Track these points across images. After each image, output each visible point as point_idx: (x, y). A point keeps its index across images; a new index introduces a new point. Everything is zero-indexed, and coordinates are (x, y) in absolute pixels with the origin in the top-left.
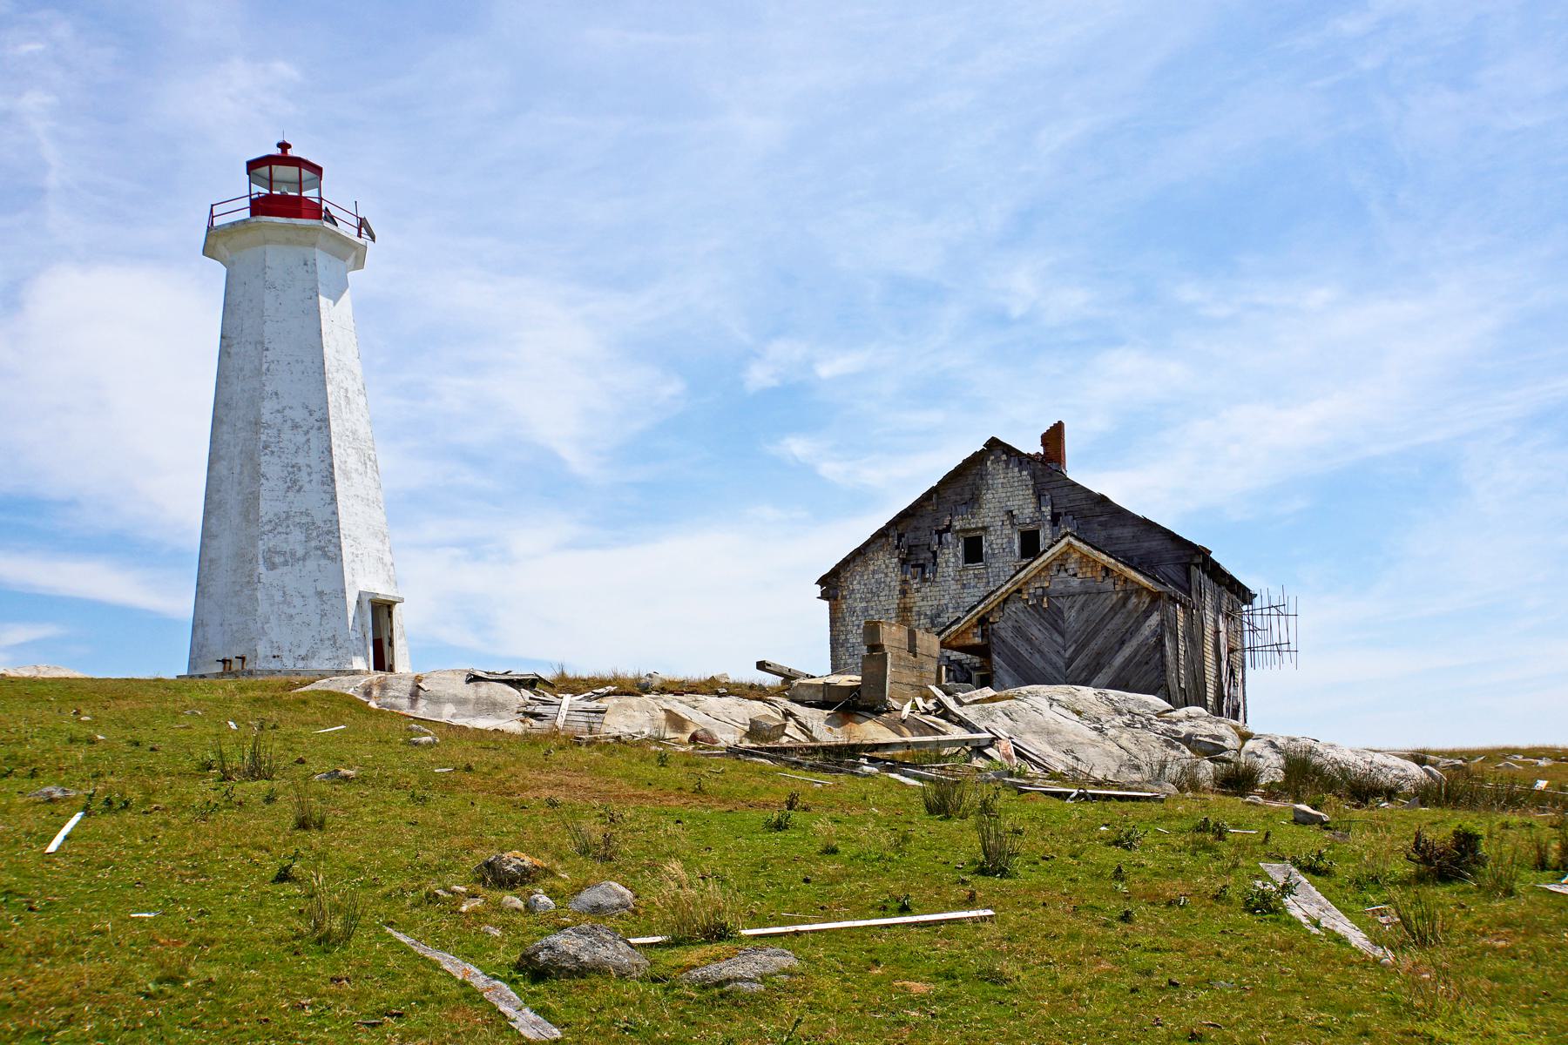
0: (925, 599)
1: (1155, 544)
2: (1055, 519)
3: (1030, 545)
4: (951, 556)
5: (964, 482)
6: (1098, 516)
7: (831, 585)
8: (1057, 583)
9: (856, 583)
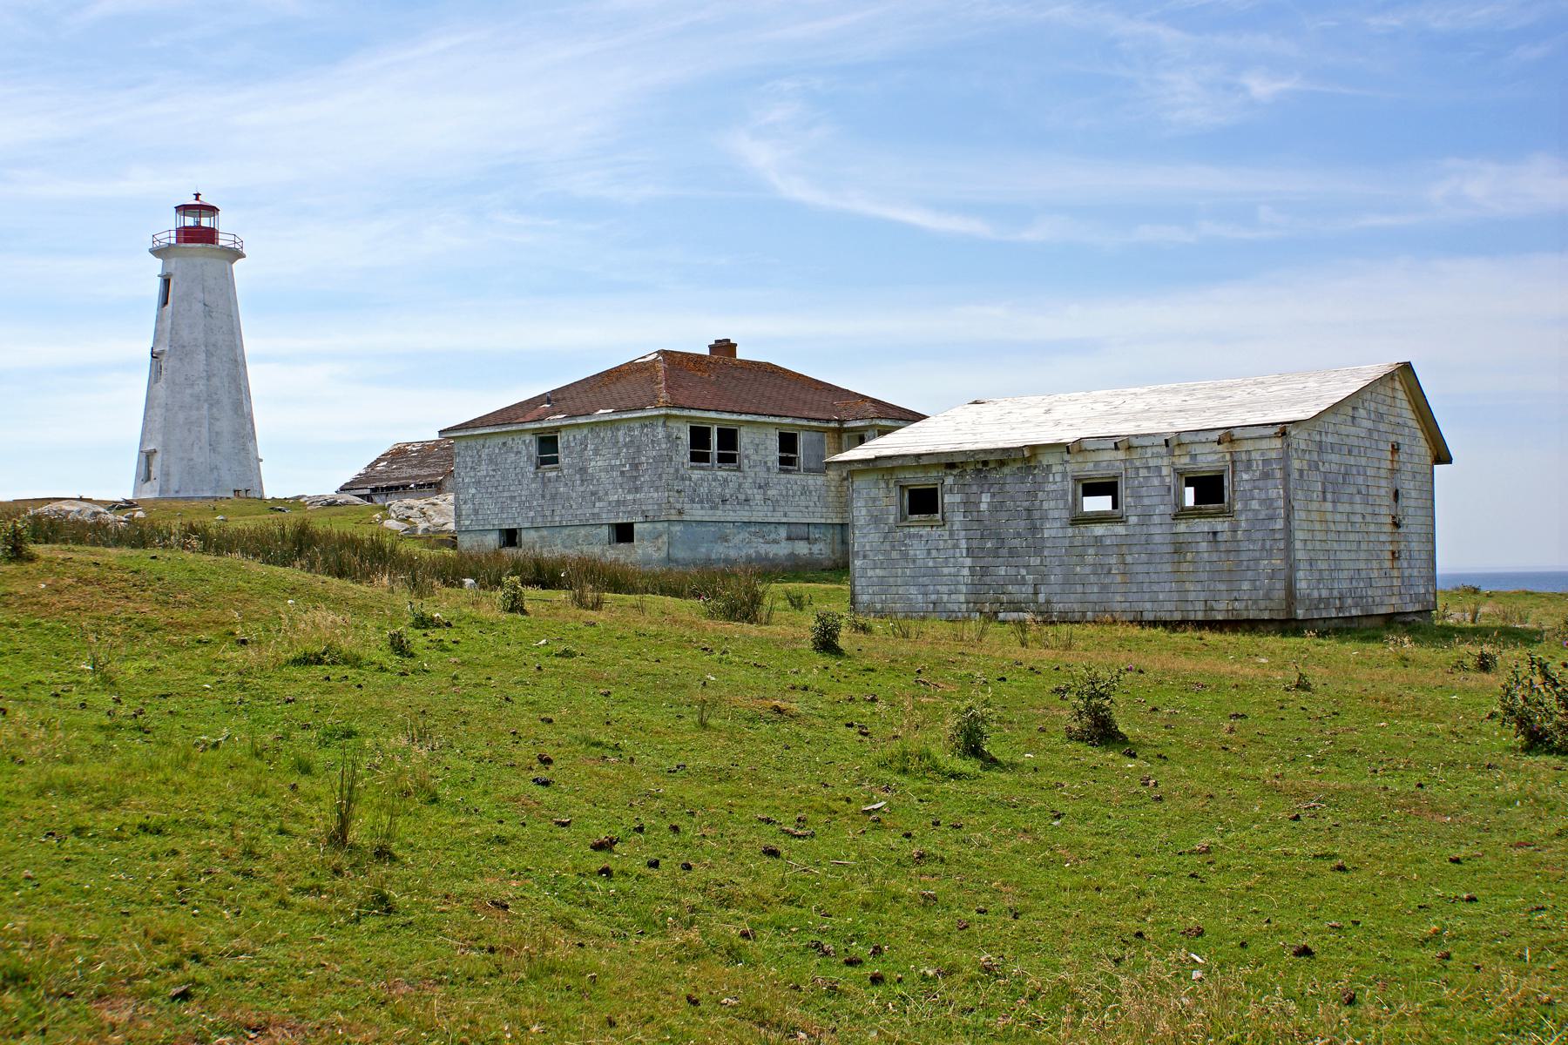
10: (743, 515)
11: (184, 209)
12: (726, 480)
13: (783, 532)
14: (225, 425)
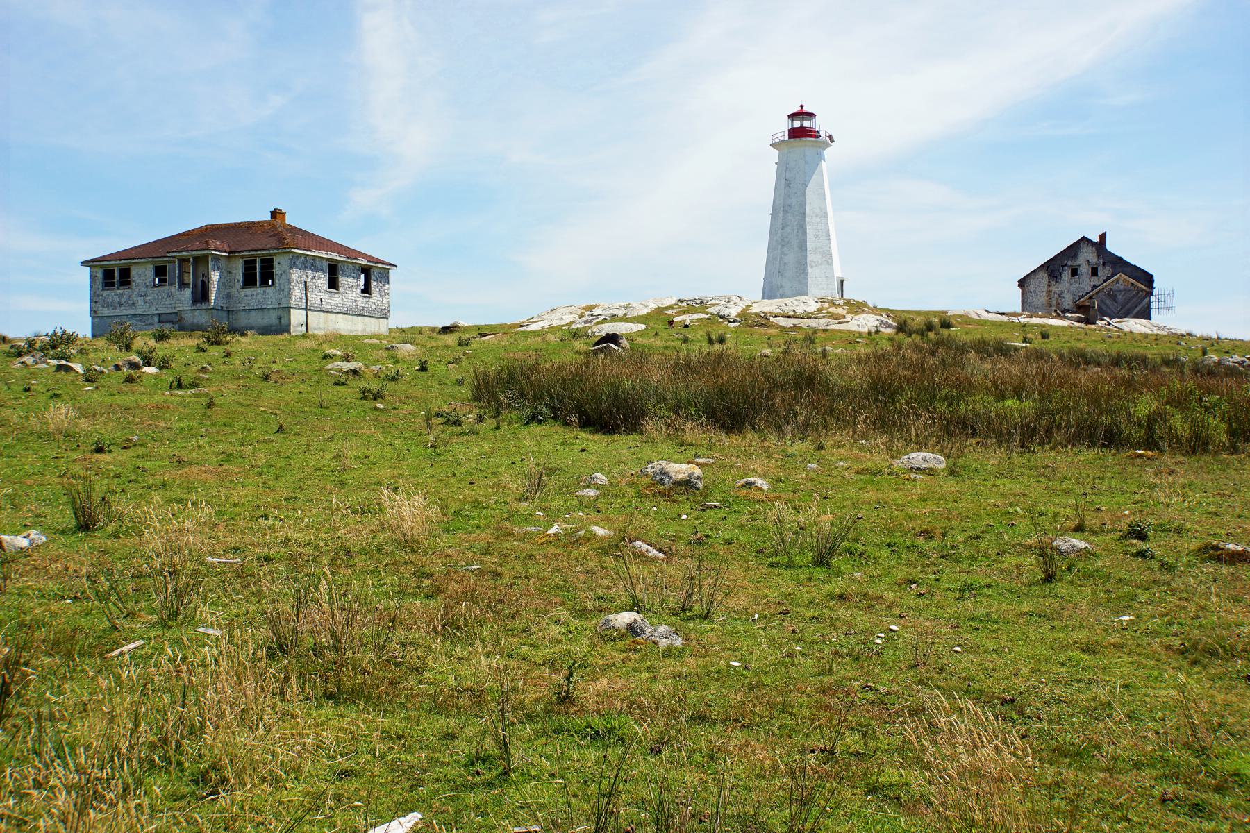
0: (1057, 288)
1: (1138, 274)
2: (1104, 264)
3: (1094, 272)
4: (1066, 275)
5: (1073, 251)
6: (1118, 264)
7: (1022, 283)
8: (1115, 287)
9: (1032, 282)
10: (132, 311)
11: (792, 116)
12: (122, 295)
13: (156, 319)
14: (791, 258)
